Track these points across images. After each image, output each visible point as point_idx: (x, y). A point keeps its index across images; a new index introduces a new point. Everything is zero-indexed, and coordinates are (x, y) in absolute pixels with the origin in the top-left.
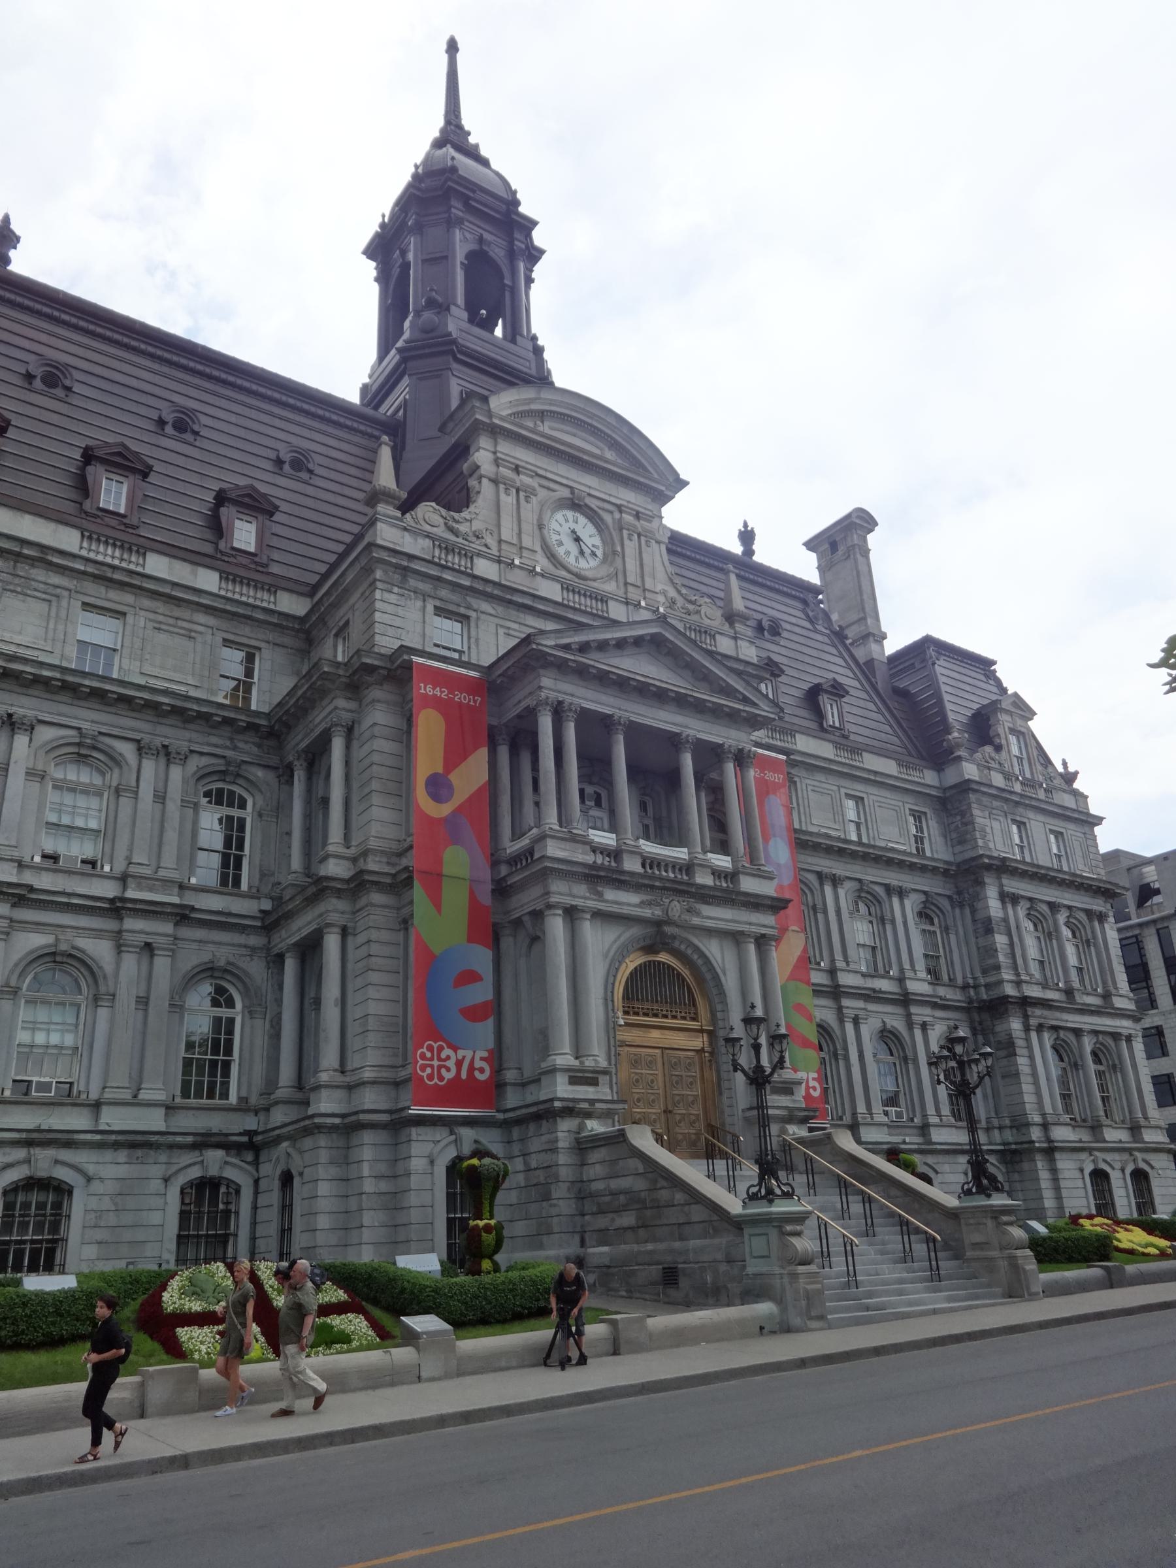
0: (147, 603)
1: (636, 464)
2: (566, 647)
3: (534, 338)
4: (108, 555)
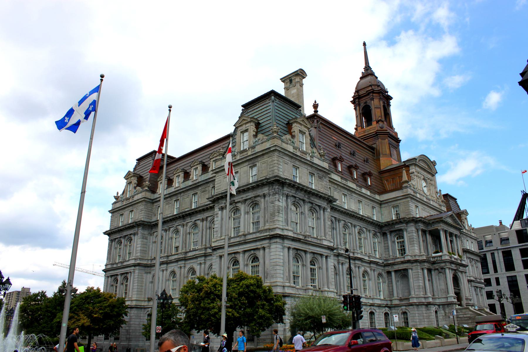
0: (364, 199)
1: (430, 169)
4: (358, 189)
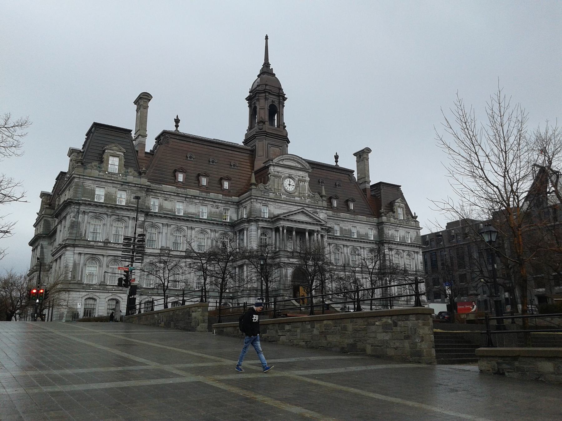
2: (285, 217)
3: (284, 123)
